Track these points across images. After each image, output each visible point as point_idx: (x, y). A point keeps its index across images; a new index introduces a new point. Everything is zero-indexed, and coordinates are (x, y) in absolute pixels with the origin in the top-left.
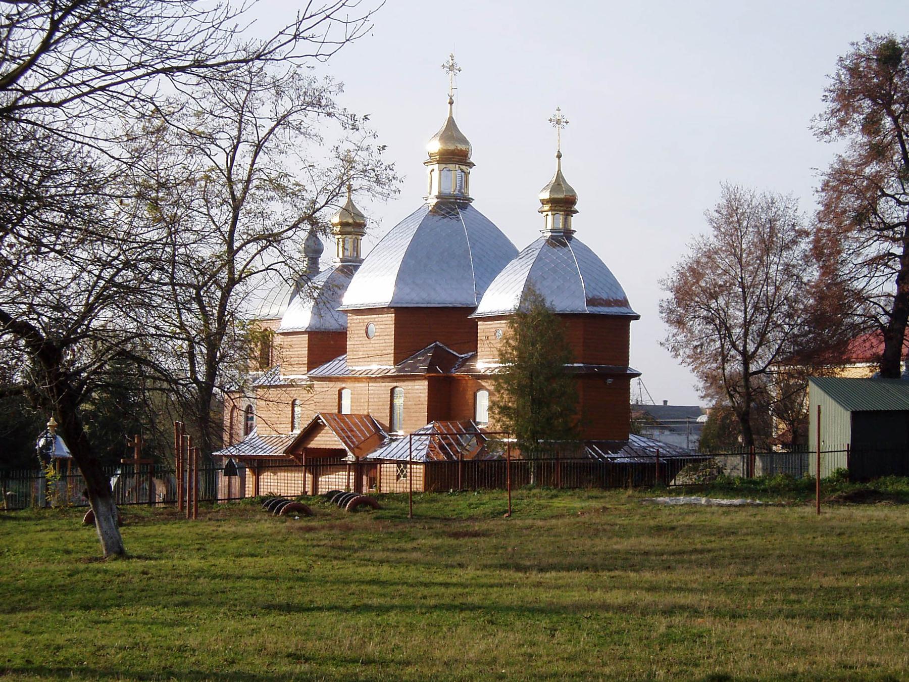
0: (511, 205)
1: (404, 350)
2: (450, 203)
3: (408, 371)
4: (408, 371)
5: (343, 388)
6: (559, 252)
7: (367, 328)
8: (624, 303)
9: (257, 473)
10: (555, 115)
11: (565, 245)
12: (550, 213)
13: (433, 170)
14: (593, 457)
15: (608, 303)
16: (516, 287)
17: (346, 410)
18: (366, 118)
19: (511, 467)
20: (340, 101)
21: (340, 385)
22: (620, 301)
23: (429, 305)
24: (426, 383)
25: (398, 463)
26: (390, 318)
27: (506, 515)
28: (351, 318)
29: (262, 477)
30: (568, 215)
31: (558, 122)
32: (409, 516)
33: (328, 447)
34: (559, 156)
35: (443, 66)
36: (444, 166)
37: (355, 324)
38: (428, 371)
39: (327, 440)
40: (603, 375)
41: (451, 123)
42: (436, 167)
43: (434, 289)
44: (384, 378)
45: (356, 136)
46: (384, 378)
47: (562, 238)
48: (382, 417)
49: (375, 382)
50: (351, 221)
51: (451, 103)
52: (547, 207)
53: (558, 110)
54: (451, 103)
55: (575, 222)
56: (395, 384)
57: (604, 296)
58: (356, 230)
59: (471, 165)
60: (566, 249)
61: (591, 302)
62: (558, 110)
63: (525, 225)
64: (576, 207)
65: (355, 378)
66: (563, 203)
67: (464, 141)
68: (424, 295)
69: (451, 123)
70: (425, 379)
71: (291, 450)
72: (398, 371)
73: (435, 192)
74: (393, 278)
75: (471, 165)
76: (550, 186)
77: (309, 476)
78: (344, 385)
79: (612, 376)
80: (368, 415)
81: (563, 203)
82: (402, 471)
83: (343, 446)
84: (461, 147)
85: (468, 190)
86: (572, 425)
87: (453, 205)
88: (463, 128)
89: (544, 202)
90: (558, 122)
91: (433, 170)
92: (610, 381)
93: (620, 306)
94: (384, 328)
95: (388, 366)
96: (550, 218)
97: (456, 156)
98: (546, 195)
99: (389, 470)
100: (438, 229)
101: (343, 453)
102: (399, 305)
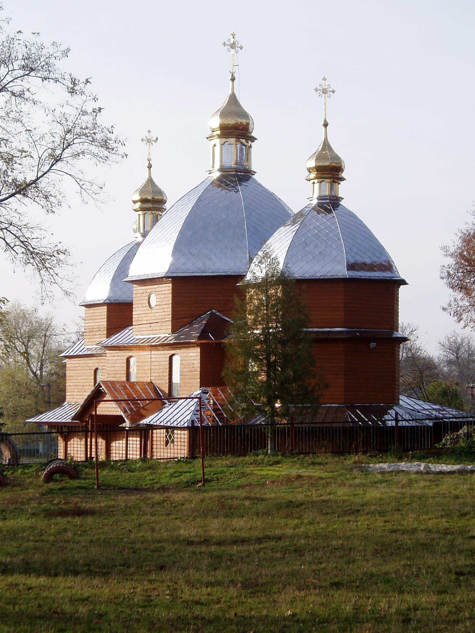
0: (284, 173)
1: (180, 318)
2: (231, 175)
3: (182, 339)
4: (182, 339)
5: (131, 357)
6: (323, 218)
7: (149, 298)
8: (388, 266)
9: (66, 440)
10: (321, 85)
11: (330, 211)
12: (316, 181)
13: (215, 145)
14: (353, 421)
15: (371, 267)
16: (282, 252)
17: (133, 379)
18: (87, 81)
19: (278, 431)
20: (62, 66)
21: (127, 354)
22: (383, 265)
23: (203, 274)
24: (198, 350)
25: (167, 428)
26: (167, 288)
27: (200, 484)
28: (137, 289)
29: (69, 443)
30: (334, 182)
31: (325, 91)
32: (96, 487)
33: (114, 414)
34: (326, 125)
35: (225, 44)
36: (224, 140)
37: (138, 295)
38: (199, 338)
39: (107, 408)
40: (365, 339)
41: (233, 99)
42: (217, 141)
43: (210, 259)
44: (163, 346)
45: (77, 100)
46: (163, 346)
47: (330, 204)
48: (162, 384)
49: (157, 350)
50: (150, 198)
51: (233, 80)
52: (313, 175)
53: (324, 79)
54: (233, 80)
55: (343, 190)
56: (173, 352)
57: (368, 261)
58: (156, 206)
59: (253, 139)
60: (330, 216)
61: (351, 267)
62: (324, 79)
63: (299, 193)
64: (343, 175)
65: (139, 346)
66: (330, 171)
67: (245, 115)
68: (199, 264)
69: (233, 99)
70: (198, 346)
71: (80, 416)
72: (176, 338)
73: (217, 166)
74: (171, 248)
75: (253, 139)
76: (316, 154)
77: (102, 442)
78: (130, 354)
79: (374, 340)
80: (151, 382)
81: (330, 171)
82: (170, 437)
83: (122, 413)
84: (244, 121)
85: (250, 164)
86: (310, 389)
87: (237, 176)
88: (246, 105)
89: (310, 170)
90: (325, 91)
91: (215, 145)
92: (373, 345)
93: (383, 271)
94: (162, 298)
95: (165, 332)
96: (317, 186)
97: (237, 130)
98: (312, 164)
99: (159, 435)
100: (216, 201)
101: (120, 419)
102: (175, 275)
